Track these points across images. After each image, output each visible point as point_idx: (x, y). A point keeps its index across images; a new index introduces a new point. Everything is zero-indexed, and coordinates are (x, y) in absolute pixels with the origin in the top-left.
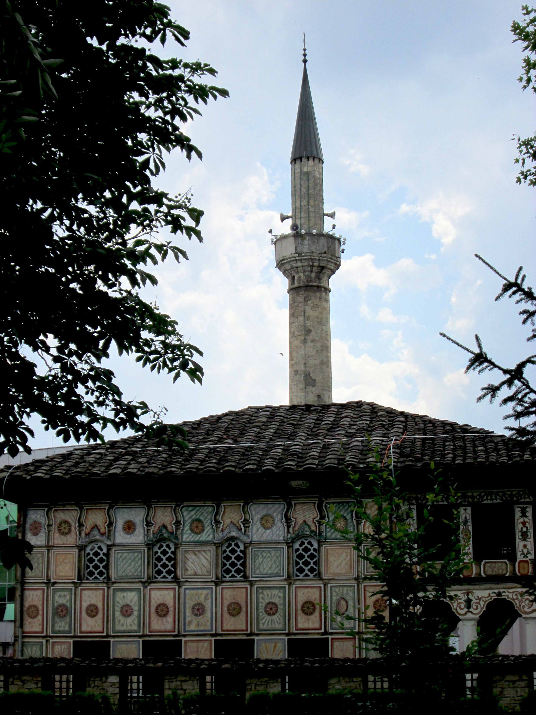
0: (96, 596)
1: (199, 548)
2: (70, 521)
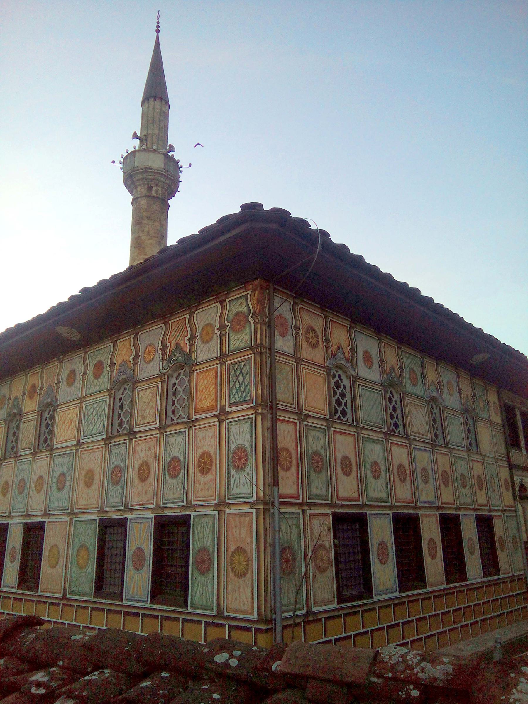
1: (417, 402)
2: (317, 330)
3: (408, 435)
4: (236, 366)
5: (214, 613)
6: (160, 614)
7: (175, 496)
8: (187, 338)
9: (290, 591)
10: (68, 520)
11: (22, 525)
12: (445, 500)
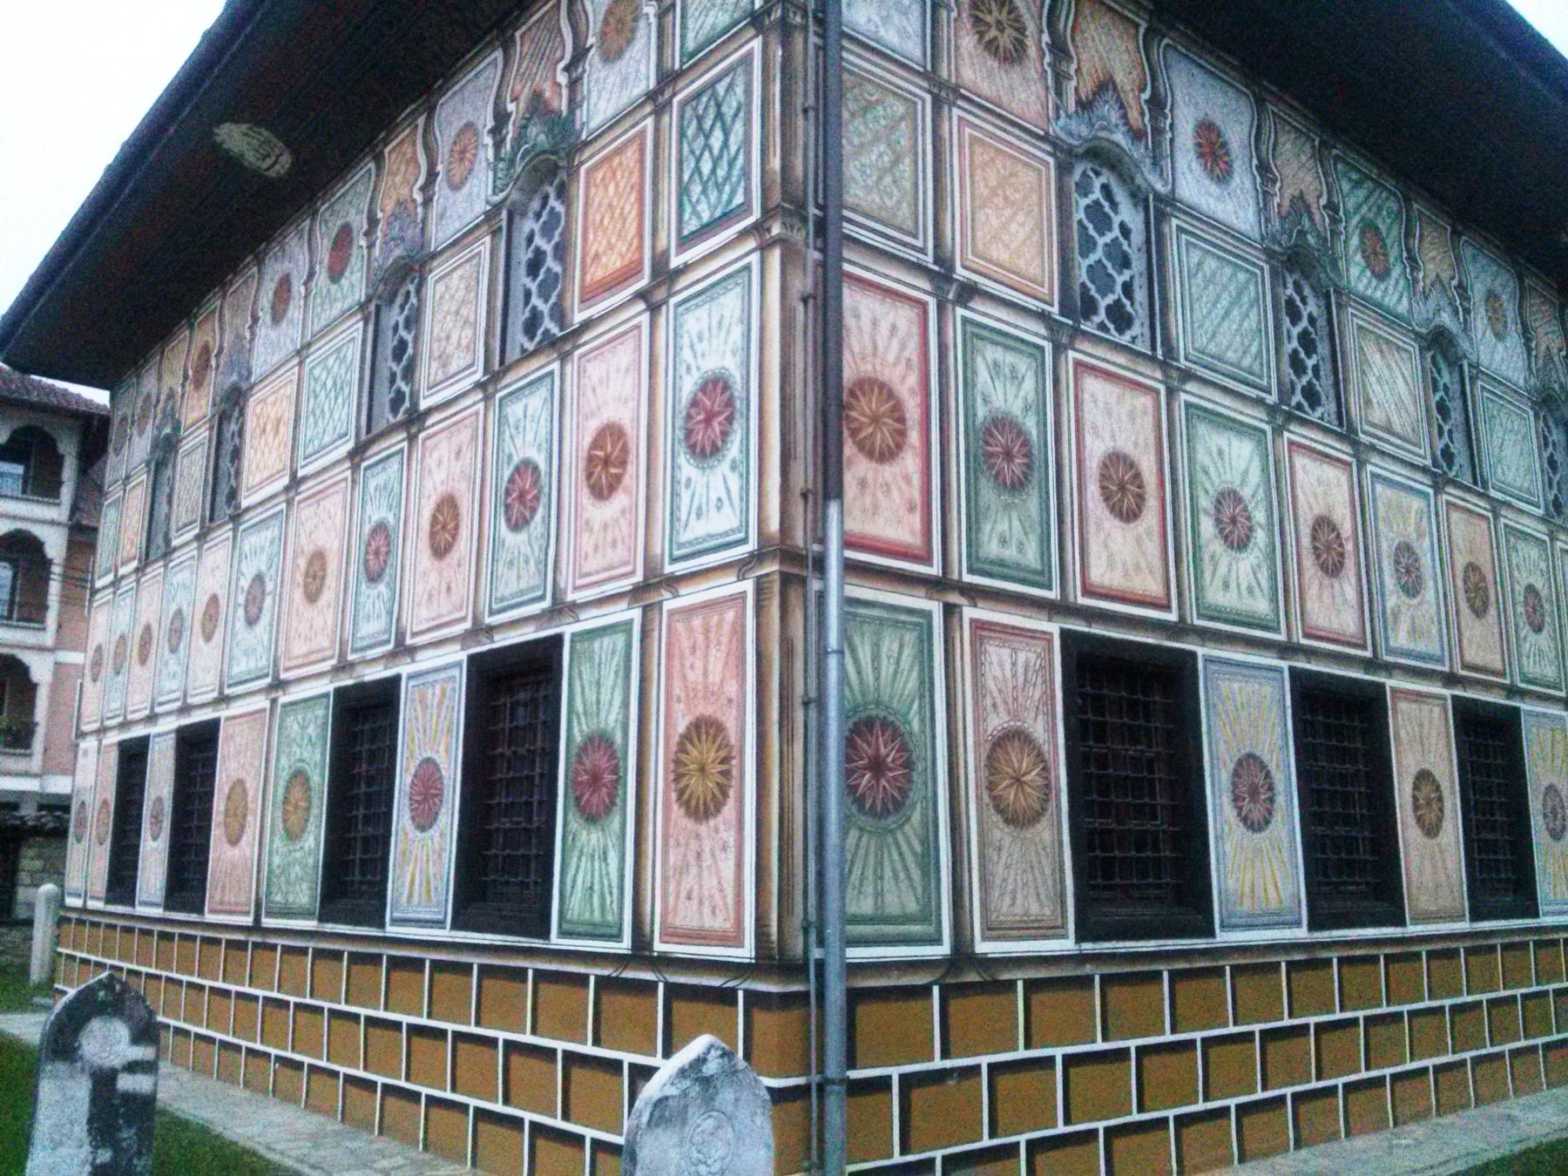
0: (1132, 415)
1: (1384, 331)
3: (1352, 430)
4: (704, 99)
5: (624, 946)
6: (476, 960)
7: (523, 585)
8: (561, 65)
9: (888, 874)
10: (267, 704)
11: (173, 735)
12: (1472, 656)
